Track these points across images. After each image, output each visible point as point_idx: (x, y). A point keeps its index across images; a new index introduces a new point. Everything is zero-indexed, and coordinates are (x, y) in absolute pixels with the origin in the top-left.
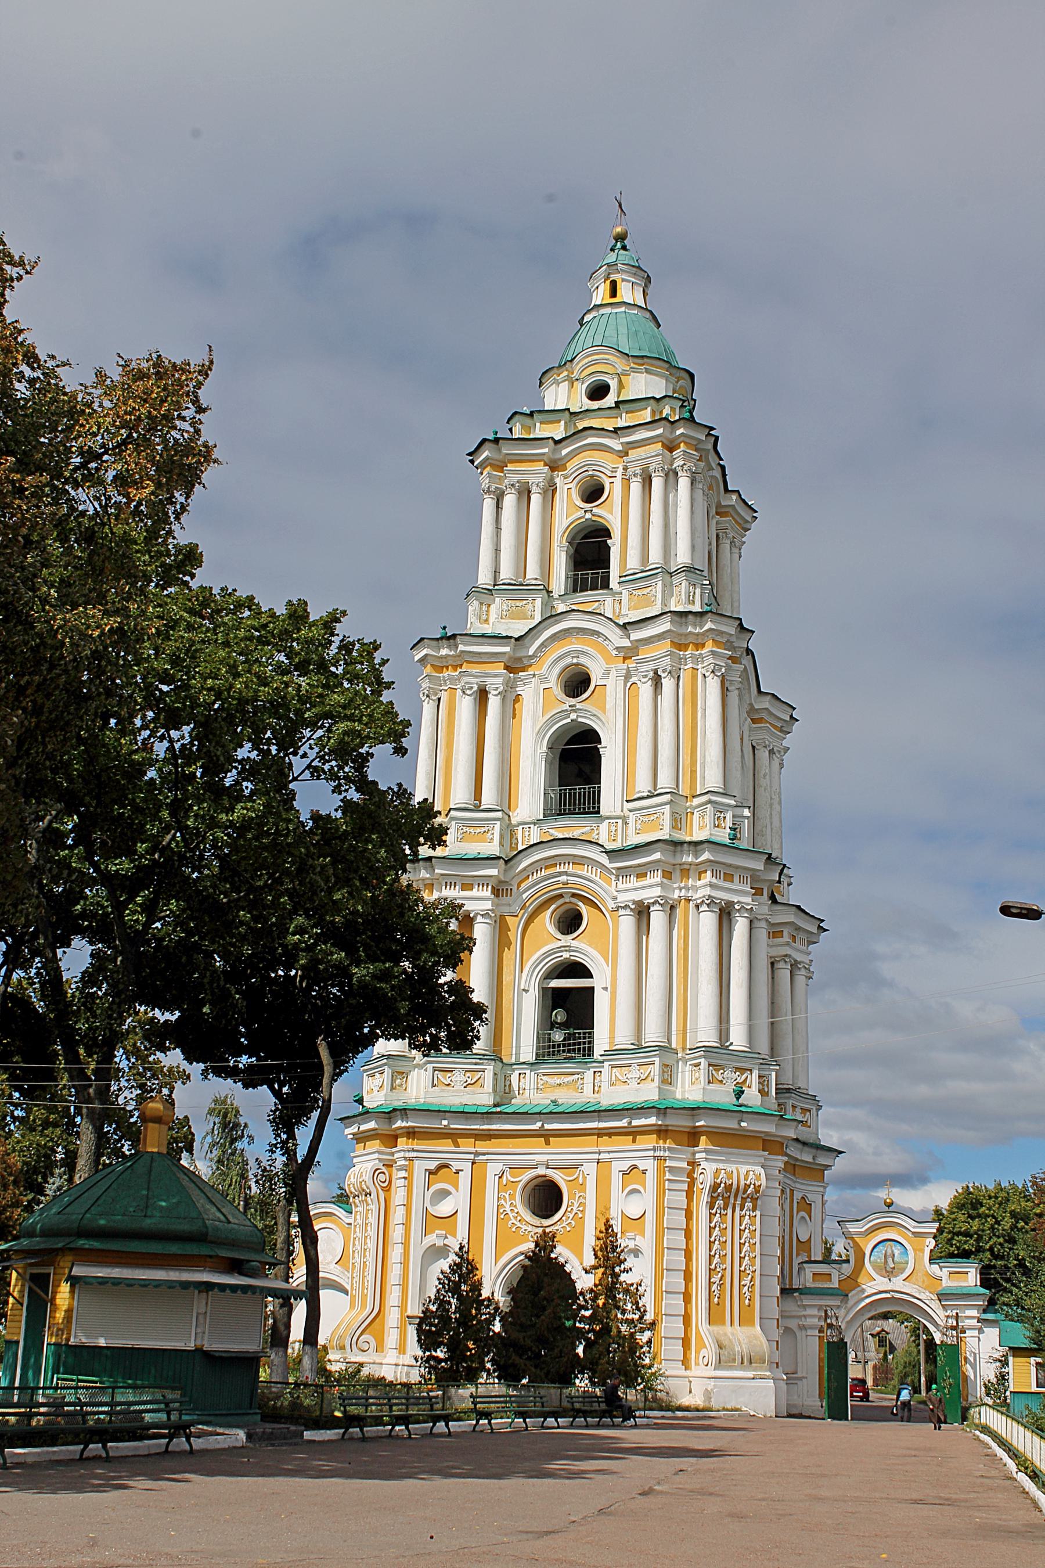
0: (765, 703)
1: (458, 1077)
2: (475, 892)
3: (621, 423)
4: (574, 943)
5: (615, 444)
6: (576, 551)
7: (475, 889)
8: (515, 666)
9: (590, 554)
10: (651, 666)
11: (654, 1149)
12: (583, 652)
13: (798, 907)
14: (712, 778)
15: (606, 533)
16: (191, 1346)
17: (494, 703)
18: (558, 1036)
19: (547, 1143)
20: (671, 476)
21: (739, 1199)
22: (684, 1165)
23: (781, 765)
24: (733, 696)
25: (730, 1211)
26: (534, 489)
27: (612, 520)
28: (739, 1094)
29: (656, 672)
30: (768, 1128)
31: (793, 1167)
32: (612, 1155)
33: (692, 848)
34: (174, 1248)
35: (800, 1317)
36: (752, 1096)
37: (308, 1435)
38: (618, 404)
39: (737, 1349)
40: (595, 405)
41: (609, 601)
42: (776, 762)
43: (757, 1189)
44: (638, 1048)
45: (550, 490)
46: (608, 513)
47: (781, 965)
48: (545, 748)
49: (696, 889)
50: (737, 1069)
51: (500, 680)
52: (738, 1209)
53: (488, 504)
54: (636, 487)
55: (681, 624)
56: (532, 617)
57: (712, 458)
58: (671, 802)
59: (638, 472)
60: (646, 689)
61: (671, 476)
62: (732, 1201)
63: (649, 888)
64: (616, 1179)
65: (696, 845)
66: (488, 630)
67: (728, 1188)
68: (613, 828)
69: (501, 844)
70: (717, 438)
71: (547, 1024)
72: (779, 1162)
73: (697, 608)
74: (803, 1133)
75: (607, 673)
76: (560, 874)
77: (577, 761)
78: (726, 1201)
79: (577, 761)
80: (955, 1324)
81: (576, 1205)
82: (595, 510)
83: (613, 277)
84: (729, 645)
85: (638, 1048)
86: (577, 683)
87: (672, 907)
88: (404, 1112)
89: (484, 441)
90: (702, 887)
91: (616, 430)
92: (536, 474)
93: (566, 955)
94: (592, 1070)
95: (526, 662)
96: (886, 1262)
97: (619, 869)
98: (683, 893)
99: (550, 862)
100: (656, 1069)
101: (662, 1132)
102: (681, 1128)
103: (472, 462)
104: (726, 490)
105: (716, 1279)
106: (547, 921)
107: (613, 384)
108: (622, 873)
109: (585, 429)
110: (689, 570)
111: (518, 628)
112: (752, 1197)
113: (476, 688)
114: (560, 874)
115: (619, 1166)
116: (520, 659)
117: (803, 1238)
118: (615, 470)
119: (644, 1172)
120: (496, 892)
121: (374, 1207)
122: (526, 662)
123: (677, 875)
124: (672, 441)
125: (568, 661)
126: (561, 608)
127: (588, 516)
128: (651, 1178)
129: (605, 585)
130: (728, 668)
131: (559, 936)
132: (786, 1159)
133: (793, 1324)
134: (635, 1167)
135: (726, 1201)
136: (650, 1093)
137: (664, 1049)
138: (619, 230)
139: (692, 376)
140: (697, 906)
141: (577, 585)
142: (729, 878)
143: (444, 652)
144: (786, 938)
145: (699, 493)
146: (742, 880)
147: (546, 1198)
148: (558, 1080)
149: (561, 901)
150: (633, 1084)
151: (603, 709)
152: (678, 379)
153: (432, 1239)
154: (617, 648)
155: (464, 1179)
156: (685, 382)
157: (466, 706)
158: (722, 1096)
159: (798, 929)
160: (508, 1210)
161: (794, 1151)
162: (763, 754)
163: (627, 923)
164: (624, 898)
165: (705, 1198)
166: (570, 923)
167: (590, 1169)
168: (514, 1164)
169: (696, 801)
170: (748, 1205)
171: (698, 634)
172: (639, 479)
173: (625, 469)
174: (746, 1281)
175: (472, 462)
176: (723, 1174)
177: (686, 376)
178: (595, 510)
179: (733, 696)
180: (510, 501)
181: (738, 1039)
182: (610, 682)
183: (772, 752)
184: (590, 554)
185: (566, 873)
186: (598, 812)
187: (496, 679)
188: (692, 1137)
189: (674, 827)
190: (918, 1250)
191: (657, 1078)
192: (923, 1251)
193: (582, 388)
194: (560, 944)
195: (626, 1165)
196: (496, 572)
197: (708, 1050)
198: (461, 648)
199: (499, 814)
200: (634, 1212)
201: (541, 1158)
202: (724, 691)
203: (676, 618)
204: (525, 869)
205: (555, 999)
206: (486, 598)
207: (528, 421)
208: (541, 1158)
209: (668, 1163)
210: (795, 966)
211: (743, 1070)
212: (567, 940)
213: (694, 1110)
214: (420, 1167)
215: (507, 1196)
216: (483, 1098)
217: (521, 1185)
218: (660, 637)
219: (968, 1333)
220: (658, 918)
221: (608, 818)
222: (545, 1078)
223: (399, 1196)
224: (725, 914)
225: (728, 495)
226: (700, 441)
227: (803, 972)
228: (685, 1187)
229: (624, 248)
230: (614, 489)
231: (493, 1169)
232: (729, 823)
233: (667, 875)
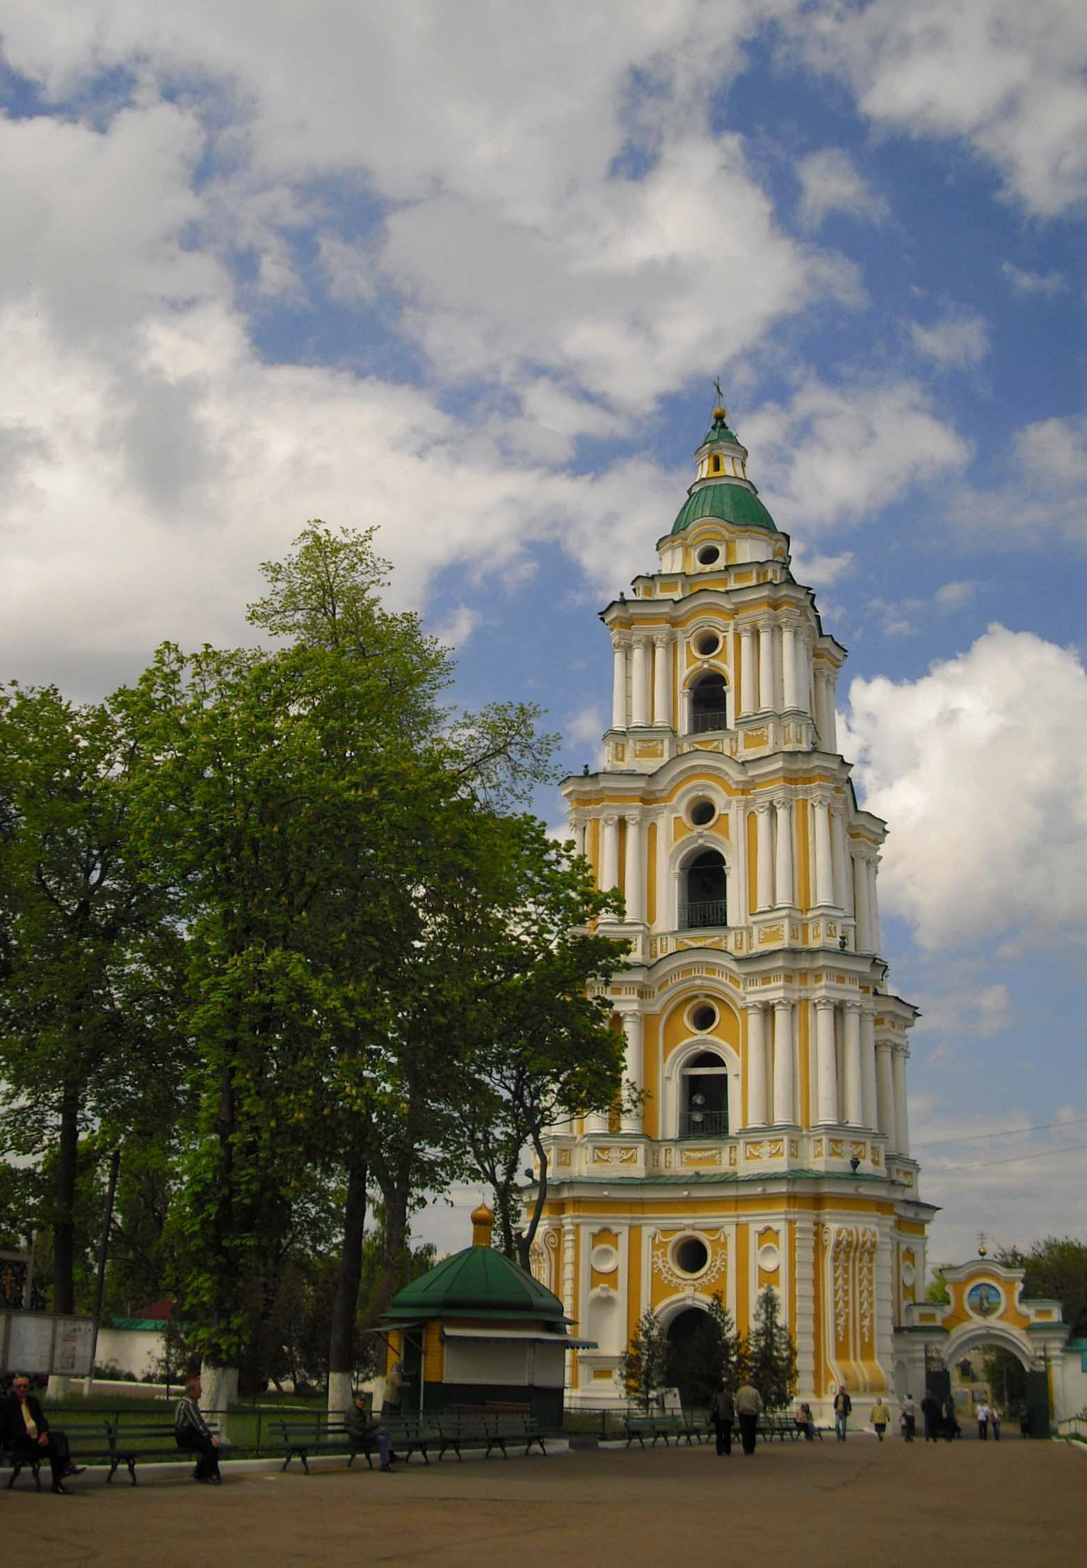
0: (863, 821)
1: (615, 1154)
2: (623, 996)
3: (733, 585)
4: (710, 1037)
5: (726, 604)
6: (696, 694)
7: (623, 991)
8: (648, 799)
9: (708, 697)
10: (767, 798)
11: (786, 1213)
12: (709, 787)
13: (897, 998)
14: (822, 896)
15: (722, 680)
16: (525, 1383)
17: (632, 832)
18: (698, 1117)
20: (776, 630)
22: (810, 1225)
23: (877, 872)
24: (838, 822)
26: (658, 644)
27: (729, 672)
28: (855, 1163)
29: (771, 803)
30: (881, 1192)
31: (901, 1223)
33: (808, 956)
34: (509, 1315)
35: (908, 1352)
36: (866, 1166)
37: (602, 1444)
38: (727, 568)
39: (861, 1379)
40: (708, 568)
41: (727, 741)
42: (873, 871)
43: (874, 1245)
44: (769, 1127)
45: (672, 645)
47: (883, 1049)
48: (677, 870)
49: (814, 990)
50: (853, 1143)
51: (637, 812)
53: (618, 657)
54: (746, 641)
56: (662, 755)
57: (811, 614)
58: (789, 916)
59: (748, 627)
60: (762, 820)
61: (776, 630)
62: (852, 1255)
63: (775, 992)
64: (753, 1239)
65: (813, 953)
66: (623, 766)
68: (739, 938)
69: (643, 953)
70: (814, 596)
71: (688, 1105)
72: (890, 1220)
73: (805, 747)
74: (908, 1194)
75: (728, 804)
76: (695, 978)
77: (704, 879)
78: (847, 1254)
79: (704, 879)
80: (1042, 1354)
82: (712, 661)
83: (716, 452)
84: (834, 778)
85: (769, 1127)
86: (703, 812)
87: (794, 1006)
88: (571, 1184)
89: (614, 602)
90: (820, 990)
91: (727, 592)
92: (660, 632)
93: (702, 1048)
95: (658, 794)
96: (981, 1304)
97: (746, 974)
98: (803, 994)
99: (686, 969)
100: (784, 1146)
101: (792, 1198)
102: (808, 1194)
103: (603, 619)
104: (821, 635)
105: (841, 1321)
107: (722, 550)
108: (750, 978)
109: (701, 591)
110: (797, 713)
111: (650, 765)
112: (871, 1250)
113: (616, 818)
114: (695, 978)
115: (755, 1227)
116: (652, 792)
117: (908, 1282)
118: (727, 626)
119: (777, 1233)
120: (641, 994)
121: (546, 1265)
122: (658, 794)
123: (797, 979)
124: (776, 600)
125: (695, 793)
126: (686, 749)
127: (706, 666)
128: (783, 1238)
129: (720, 724)
130: (834, 798)
131: (696, 1031)
132: (895, 1217)
133: (904, 1358)
134: (769, 1229)
135: (847, 1254)
136: (781, 1165)
137: (791, 1128)
138: (718, 410)
139: (787, 538)
140: (815, 1005)
141: (699, 725)
142: (841, 979)
143: (588, 788)
144: (887, 1025)
145: (801, 645)
146: (852, 981)
147: (693, 1255)
148: (699, 1155)
149: (695, 1002)
150: (766, 1158)
151: (727, 835)
152: (777, 541)
153: (597, 1291)
154: (737, 783)
155: (623, 1241)
156: (782, 544)
157: (608, 835)
158: (841, 1165)
159: (897, 1016)
160: (661, 1265)
161: (900, 1210)
162: (861, 866)
163: (754, 1021)
164: (751, 999)
165: (829, 1254)
166: (704, 1018)
167: (731, 1230)
168: (663, 1227)
169: (810, 915)
170: (866, 1257)
171: (805, 770)
173: (737, 625)
174: (866, 1322)
175: (603, 619)
176: (844, 1233)
177: (782, 537)
178: (712, 661)
179: (838, 822)
180: (638, 654)
181: (854, 1120)
183: (868, 862)
184: (708, 697)
185: (700, 977)
186: (725, 924)
187: (633, 812)
188: (818, 1201)
189: (793, 936)
190: (1009, 1293)
191: (785, 1154)
192: (1012, 1293)
193: (695, 554)
194: (695, 1038)
195: (760, 1227)
196: (628, 716)
197: (828, 1127)
198: (602, 784)
199: (641, 928)
200: (769, 1265)
201: (688, 1223)
202: (831, 816)
203: (788, 758)
204: (665, 975)
205: (692, 1086)
206: (621, 739)
207: (648, 583)
208: (688, 1223)
209: (797, 1225)
210: (895, 1049)
211: (858, 1143)
212: (702, 1035)
213: (818, 1178)
214: (585, 1233)
216: (638, 1170)
217: (670, 1246)
218: (776, 771)
219: (1053, 1362)
220: (781, 1017)
221: (734, 929)
223: (568, 1256)
224: (839, 1010)
225: (823, 639)
226: (800, 600)
227: (902, 1054)
228: (813, 1244)
229: (723, 426)
230: (727, 641)
231: (647, 1232)
232: (839, 934)
233: (788, 979)
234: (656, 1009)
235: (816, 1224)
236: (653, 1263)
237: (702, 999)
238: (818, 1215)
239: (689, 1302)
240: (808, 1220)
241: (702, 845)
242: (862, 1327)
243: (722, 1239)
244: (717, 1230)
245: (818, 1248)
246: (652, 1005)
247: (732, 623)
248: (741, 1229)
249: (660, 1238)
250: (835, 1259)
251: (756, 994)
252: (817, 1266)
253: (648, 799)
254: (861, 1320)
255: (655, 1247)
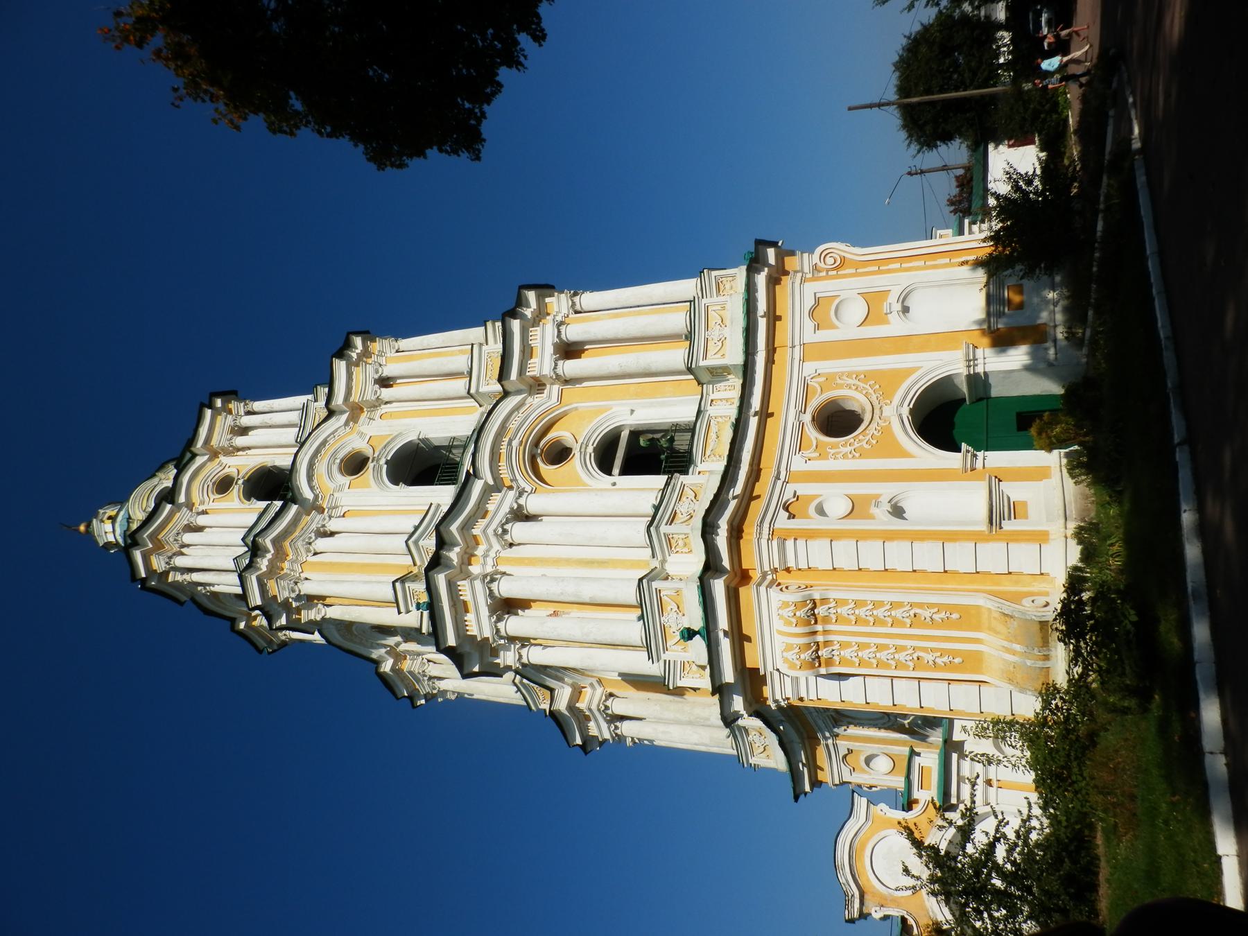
1: (683, 508)
4: (580, 442)
12: (335, 452)
19: (772, 415)
32: (797, 342)
75: (361, 434)
81: (850, 381)
86: (355, 465)
93: (590, 449)
94: (709, 407)
119: (817, 301)
134: (812, 313)
147: (837, 421)
150: (726, 332)
166: (560, 454)
195: (809, 324)
201: (791, 415)
215: (833, 451)
222: (708, 453)
231: (798, 464)
236: (845, 456)
239: (905, 412)
241: (387, 463)
243: (822, 379)
244: (807, 387)
248: (811, 352)
249: (807, 453)
251: (543, 363)
255: (822, 456)
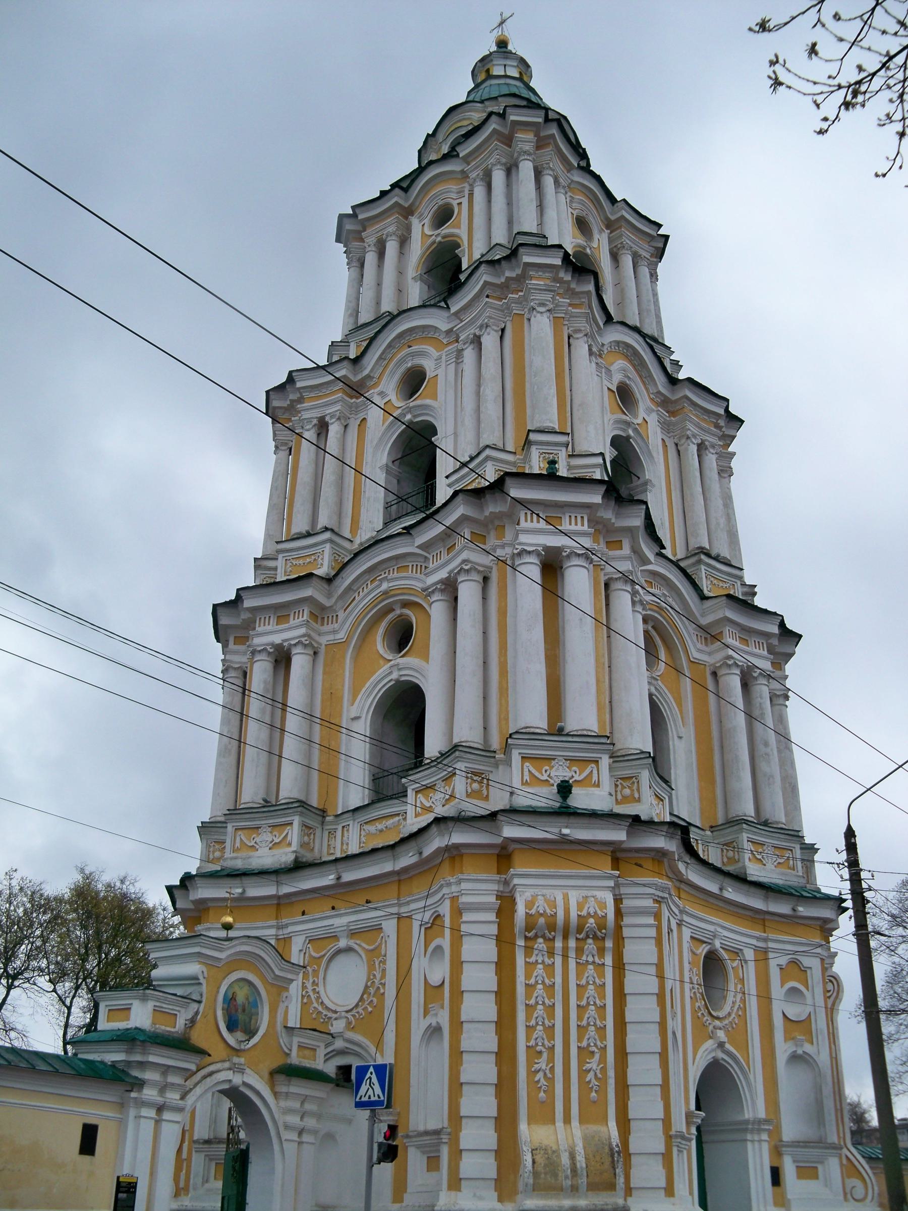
8: (356, 390)
21: (572, 943)
25: (558, 960)
27: (462, 233)
28: (565, 789)
30: (619, 835)
46: (458, 229)
52: (572, 954)
55: (498, 276)
62: (559, 944)
67: (552, 927)
93: (395, 676)
106: (379, 644)
116: (363, 382)
127: (439, 239)
149: (391, 616)
163: (438, 610)
166: (402, 637)
167: (390, 927)
172: (478, 183)
182: (441, 372)
204: (349, 589)
216: (285, 856)
228: (493, 929)
234: (341, 635)
235: (498, 897)
237: (398, 612)
238: (506, 883)
240: (486, 893)
242: (583, 1073)
245: (504, 939)
246: (335, 632)
247: (466, 185)
250: (529, 950)
252: (504, 967)
253: (356, 390)
254: (581, 1063)
